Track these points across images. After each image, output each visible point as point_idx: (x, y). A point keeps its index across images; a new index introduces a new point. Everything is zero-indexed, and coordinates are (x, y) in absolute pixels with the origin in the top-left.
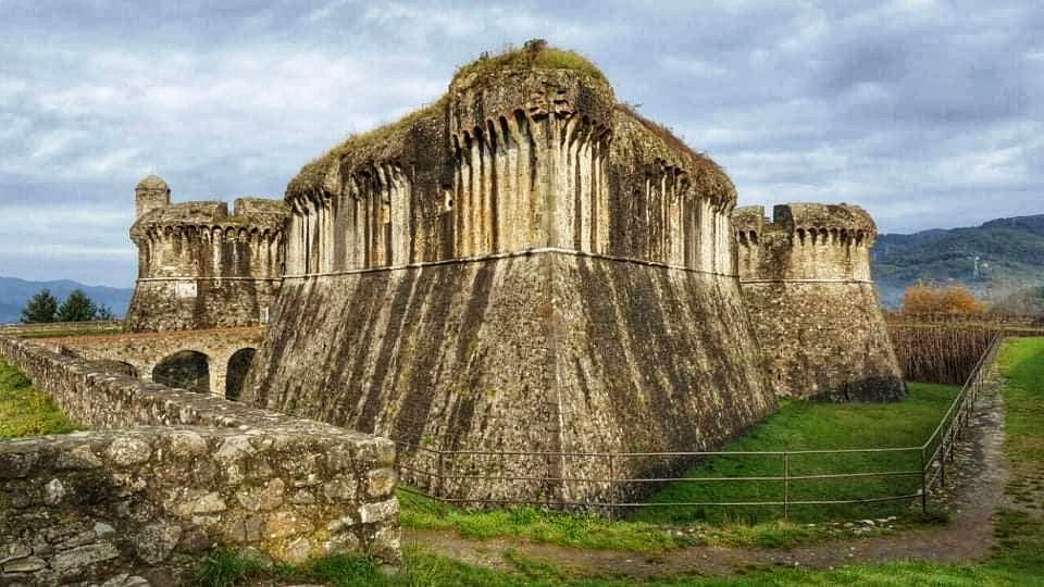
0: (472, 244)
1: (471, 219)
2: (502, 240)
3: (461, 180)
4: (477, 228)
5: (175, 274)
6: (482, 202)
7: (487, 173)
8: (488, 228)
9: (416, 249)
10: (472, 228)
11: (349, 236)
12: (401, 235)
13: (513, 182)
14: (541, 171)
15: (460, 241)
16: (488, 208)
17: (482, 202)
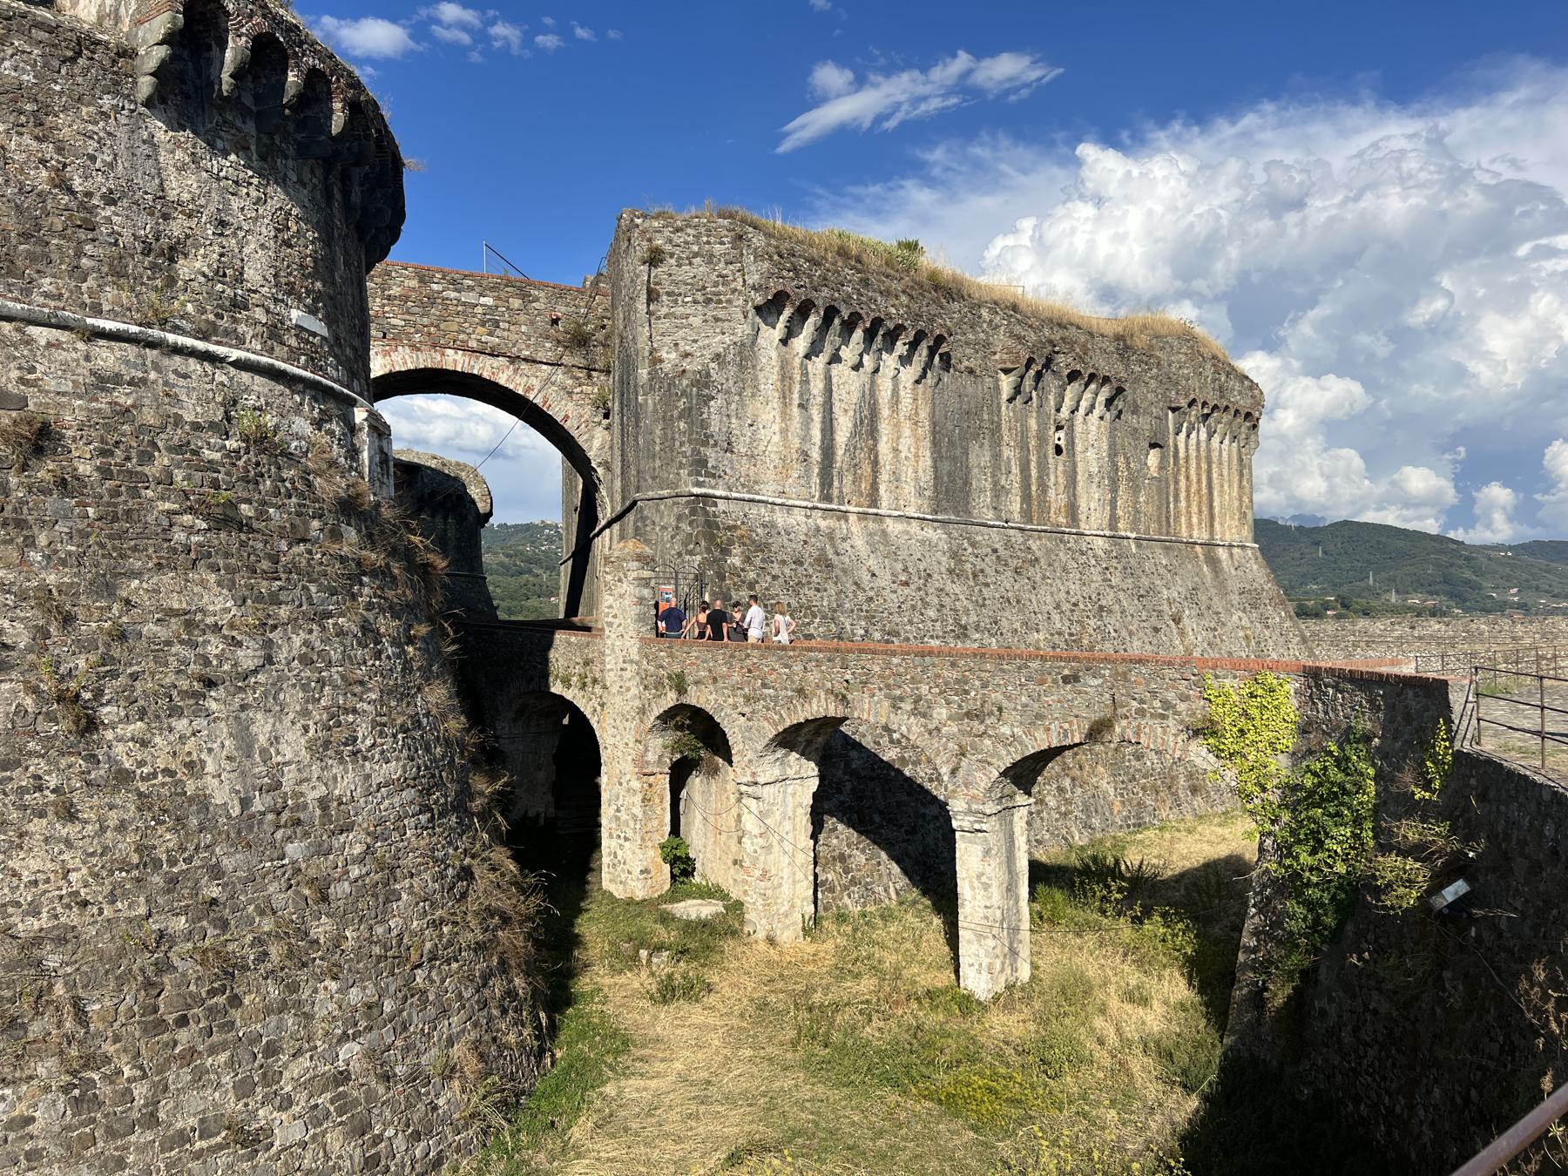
0: (1190, 526)
1: (1188, 496)
2: (1217, 527)
3: (1176, 446)
4: (1194, 509)
6: (1199, 481)
7: (1203, 454)
8: (1205, 509)
9: (1120, 512)
10: (1189, 506)
11: (979, 456)
12: (1094, 486)
13: (1225, 473)
14: (1246, 471)
15: (1177, 518)
16: (1204, 491)
17: (1199, 481)
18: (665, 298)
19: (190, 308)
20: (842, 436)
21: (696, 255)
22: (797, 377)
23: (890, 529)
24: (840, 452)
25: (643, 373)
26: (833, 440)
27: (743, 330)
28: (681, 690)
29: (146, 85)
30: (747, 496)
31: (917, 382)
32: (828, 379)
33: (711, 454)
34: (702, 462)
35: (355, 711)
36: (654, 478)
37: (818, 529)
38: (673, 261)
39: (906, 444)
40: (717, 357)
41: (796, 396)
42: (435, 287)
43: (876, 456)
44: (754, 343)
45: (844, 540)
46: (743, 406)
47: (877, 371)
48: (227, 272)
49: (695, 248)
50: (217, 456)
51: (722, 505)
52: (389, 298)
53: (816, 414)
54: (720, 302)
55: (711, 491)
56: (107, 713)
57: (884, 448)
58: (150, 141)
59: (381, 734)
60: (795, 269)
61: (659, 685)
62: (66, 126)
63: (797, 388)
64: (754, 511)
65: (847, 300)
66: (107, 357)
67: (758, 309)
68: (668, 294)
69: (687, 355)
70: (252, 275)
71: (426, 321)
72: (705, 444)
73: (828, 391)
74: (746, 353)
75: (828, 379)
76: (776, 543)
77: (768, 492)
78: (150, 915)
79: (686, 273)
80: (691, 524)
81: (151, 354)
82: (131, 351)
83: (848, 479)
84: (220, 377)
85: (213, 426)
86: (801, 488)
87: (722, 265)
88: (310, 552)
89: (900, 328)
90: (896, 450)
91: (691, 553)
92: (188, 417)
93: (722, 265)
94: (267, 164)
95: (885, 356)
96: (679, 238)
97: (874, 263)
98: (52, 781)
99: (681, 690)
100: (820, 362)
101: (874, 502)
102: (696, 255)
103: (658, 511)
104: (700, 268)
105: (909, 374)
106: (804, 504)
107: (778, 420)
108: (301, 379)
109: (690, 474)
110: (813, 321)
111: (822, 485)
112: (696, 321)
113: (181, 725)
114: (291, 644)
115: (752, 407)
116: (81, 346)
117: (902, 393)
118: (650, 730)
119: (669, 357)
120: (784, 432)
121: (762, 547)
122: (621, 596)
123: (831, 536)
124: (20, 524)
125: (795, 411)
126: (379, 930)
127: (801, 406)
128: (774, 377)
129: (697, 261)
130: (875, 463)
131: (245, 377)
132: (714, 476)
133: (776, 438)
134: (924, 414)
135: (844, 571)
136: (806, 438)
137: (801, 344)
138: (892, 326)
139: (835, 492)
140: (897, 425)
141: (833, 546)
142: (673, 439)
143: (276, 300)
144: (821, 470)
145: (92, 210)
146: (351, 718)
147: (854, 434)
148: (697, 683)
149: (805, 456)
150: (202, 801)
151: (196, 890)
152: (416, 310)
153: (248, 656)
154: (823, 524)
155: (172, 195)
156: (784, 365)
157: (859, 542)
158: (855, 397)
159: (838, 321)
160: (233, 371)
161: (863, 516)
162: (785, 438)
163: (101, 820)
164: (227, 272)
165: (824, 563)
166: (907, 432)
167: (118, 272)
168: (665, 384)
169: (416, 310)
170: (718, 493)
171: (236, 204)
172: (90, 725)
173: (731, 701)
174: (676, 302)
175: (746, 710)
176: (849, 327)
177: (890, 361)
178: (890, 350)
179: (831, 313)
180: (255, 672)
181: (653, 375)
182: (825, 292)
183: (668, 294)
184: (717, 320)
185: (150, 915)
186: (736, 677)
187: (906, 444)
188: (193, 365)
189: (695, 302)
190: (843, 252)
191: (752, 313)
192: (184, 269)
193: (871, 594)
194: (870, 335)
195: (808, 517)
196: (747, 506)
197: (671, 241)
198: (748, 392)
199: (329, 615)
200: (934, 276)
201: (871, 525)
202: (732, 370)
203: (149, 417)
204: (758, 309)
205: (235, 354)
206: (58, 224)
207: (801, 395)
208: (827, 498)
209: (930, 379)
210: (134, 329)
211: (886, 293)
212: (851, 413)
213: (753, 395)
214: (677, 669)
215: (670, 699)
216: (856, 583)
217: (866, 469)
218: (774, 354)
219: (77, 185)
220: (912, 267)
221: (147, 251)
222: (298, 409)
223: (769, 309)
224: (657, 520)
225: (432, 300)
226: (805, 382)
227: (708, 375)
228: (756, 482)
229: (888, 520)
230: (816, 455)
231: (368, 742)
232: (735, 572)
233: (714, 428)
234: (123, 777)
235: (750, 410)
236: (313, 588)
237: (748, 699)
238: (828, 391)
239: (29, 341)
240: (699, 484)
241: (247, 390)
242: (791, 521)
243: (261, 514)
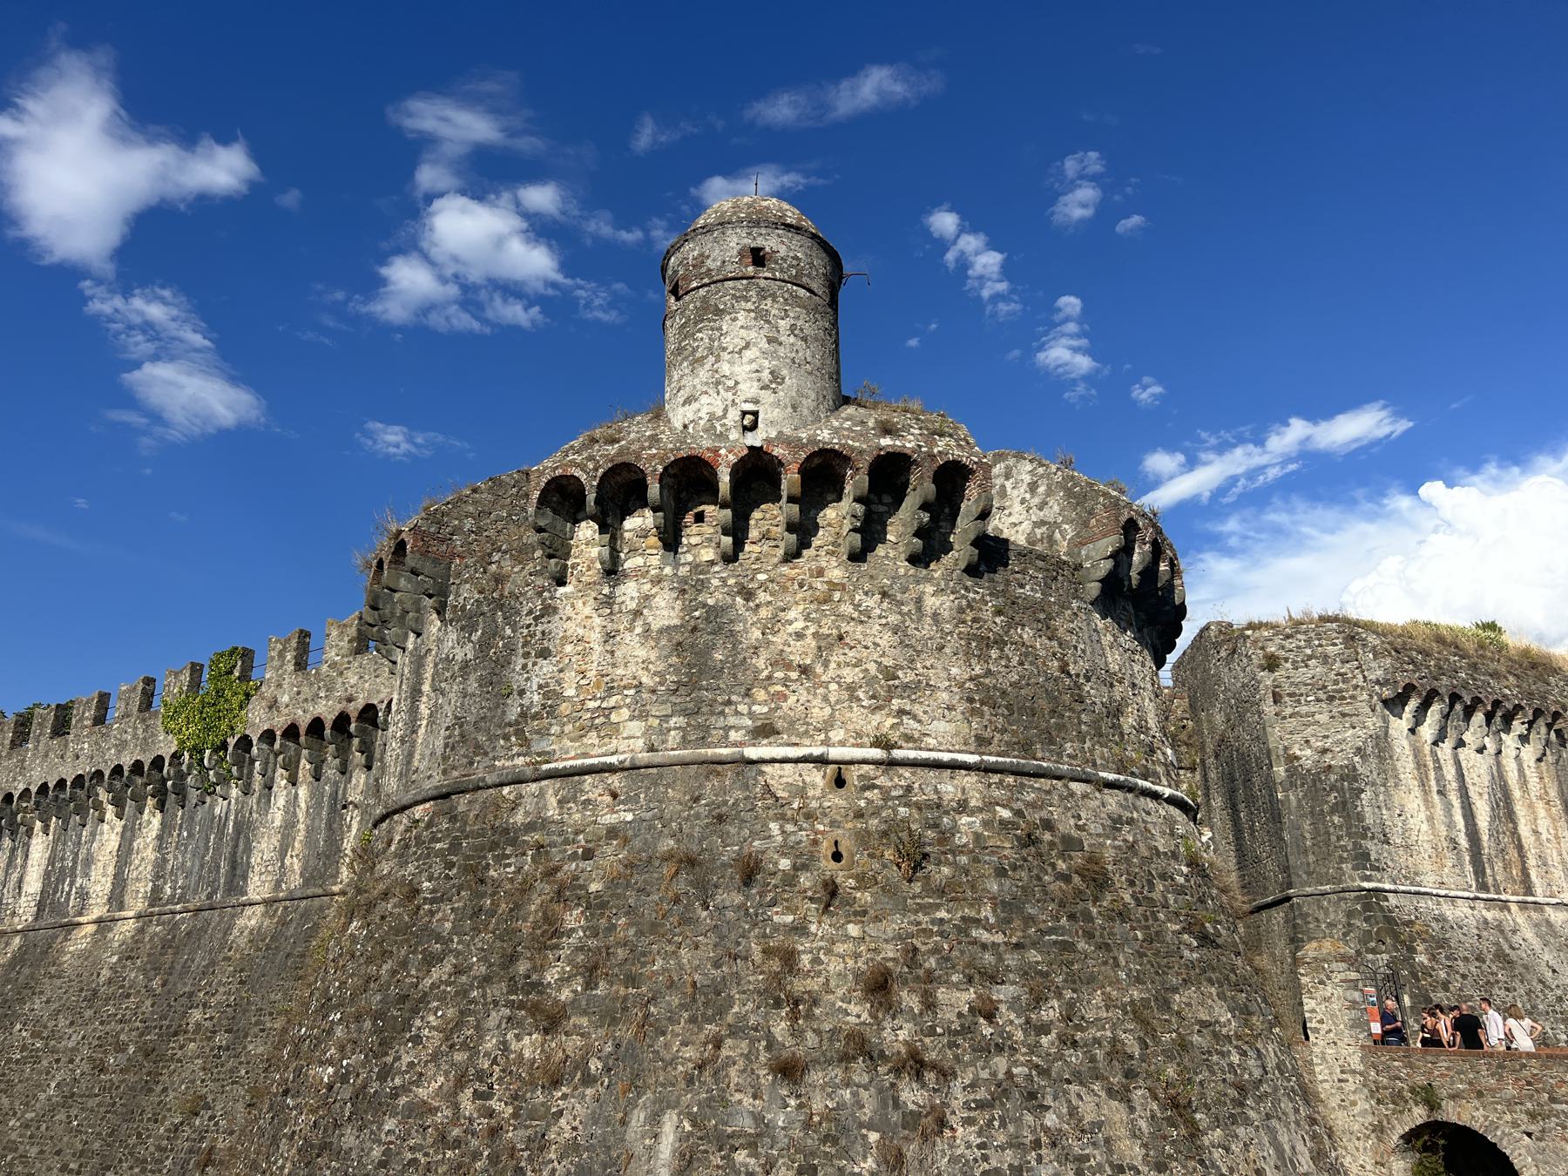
18: (1287, 699)
20: (1483, 821)
21: (1310, 658)
22: (1431, 765)
23: (1552, 918)
24: (1485, 838)
25: (1280, 771)
26: (1475, 825)
27: (1373, 723)
28: (1432, 1105)
29: (1094, 589)
30: (1413, 889)
31: (1539, 760)
32: (1458, 763)
33: (1371, 846)
34: (1366, 856)
36: (1309, 874)
37: (1486, 922)
38: (1288, 665)
39: (1544, 825)
40: (1358, 751)
41: (1433, 783)
43: (1519, 840)
44: (1386, 734)
45: (1514, 932)
46: (1390, 796)
47: (1500, 752)
49: (1309, 651)
51: (1393, 900)
53: (1454, 798)
54: (1344, 698)
55: (1380, 885)
57: (1524, 830)
60: (1413, 662)
61: (1397, 1098)
62: (1061, 625)
63: (1432, 775)
64: (1425, 904)
65: (1465, 686)
67: (1385, 702)
68: (1290, 695)
69: (1325, 751)
72: (1364, 837)
73: (1460, 776)
74: (1382, 744)
75: (1458, 763)
76: (1454, 937)
77: (1429, 883)
79: (1303, 674)
80: (1367, 920)
83: (1499, 866)
86: (1458, 879)
87: (1338, 664)
89: (1518, 708)
90: (1536, 832)
91: (1373, 951)
93: (1338, 664)
95: (1503, 736)
96: (1286, 644)
97: (1470, 647)
99: (1432, 1105)
100: (1447, 747)
101: (1529, 890)
102: (1310, 658)
103: (1320, 907)
104: (1317, 669)
105: (1529, 753)
106: (1466, 894)
107: (1423, 808)
109: (1355, 868)
110: (1435, 710)
111: (1476, 873)
112: (1323, 718)
115: (1398, 796)
117: (1527, 772)
118: (1393, 1151)
119: (1307, 756)
120: (1430, 819)
121: (1442, 943)
122: (1325, 999)
123: (1500, 928)
124: (1107, 947)
125: (1436, 797)
127: (1439, 792)
128: (1411, 766)
129: (1312, 662)
130: (1520, 847)
132: (1378, 869)
133: (1425, 827)
134: (1553, 793)
135: (1526, 967)
136: (1451, 825)
137: (1427, 731)
138: (1510, 707)
139: (1490, 881)
140: (1531, 806)
141: (1506, 939)
142: (1328, 833)
144: (1472, 857)
145: (1079, 687)
147: (1494, 818)
148: (1453, 1097)
149: (1454, 842)
154: (1489, 915)
156: (1417, 752)
157: (1529, 934)
158: (1486, 780)
159: (1462, 705)
161: (1523, 905)
162: (1433, 826)
165: (1501, 956)
166: (1542, 813)
168: (1313, 782)
170: (1387, 886)
172: (1195, 1133)
173: (1508, 1117)
174: (1299, 701)
175: (1532, 1128)
176: (1469, 712)
177: (1510, 740)
178: (1508, 730)
179: (1455, 698)
181: (1292, 772)
182: (1445, 680)
183: (1290, 695)
184: (1344, 715)
186: (1511, 1091)
187: (1544, 825)
189: (1318, 700)
190: (1440, 640)
191: (1379, 706)
193: (1559, 992)
194: (1489, 717)
195: (1472, 908)
196: (1415, 899)
197: (1283, 648)
198: (1391, 783)
200: (1526, 653)
201: (1534, 915)
202: (1373, 761)
204: (1385, 702)
207: (1438, 781)
208: (1483, 887)
209: (1550, 758)
211: (1495, 675)
212: (1486, 797)
213: (1396, 785)
214: (1421, 1080)
215: (1419, 1115)
216: (1540, 981)
217: (1513, 854)
218: (1405, 743)
219: (1072, 669)
220: (1502, 647)
223: (1395, 704)
224: (1322, 917)
226: (1438, 768)
227: (1355, 769)
228: (1416, 874)
229: (1547, 908)
230: (1463, 842)
232: (1427, 972)
233: (1369, 821)
235: (1396, 799)
237: (1533, 1116)
238: (1460, 776)
239: (1072, 794)
240: (1368, 879)
242: (1458, 913)
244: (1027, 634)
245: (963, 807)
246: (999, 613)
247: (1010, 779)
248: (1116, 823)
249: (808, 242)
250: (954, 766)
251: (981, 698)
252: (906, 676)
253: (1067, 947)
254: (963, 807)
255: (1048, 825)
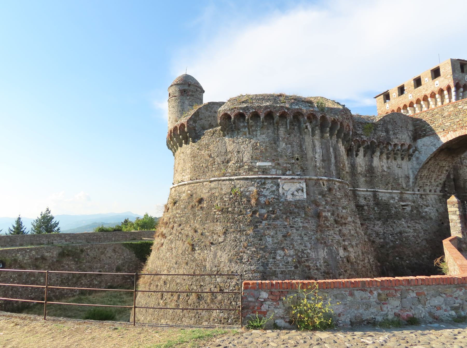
5: (273, 171)
19: (230, 171)
35: (244, 252)
42: (459, 107)
48: (240, 161)
50: (227, 199)
52: (444, 117)
56: (197, 248)
58: (225, 143)
59: (252, 259)
62: (211, 147)
66: (213, 185)
70: (245, 160)
71: (458, 120)
78: (191, 285)
81: (220, 182)
82: (217, 182)
84: (233, 183)
85: (228, 193)
88: (244, 217)
92: (223, 192)
94: (251, 134)
98: (187, 259)
108: (254, 178)
113: (206, 251)
114: (231, 237)
116: (210, 184)
126: (233, 303)
131: (238, 181)
143: (251, 163)
146: (242, 254)
150: (205, 267)
151: (200, 282)
152: (454, 117)
153: (221, 240)
155: (228, 151)
160: (235, 181)
163: (190, 266)
164: (240, 161)
167: (219, 169)
169: (454, 117)
171: (242, 147)
172: (193, 250)
180: (222, 242)
185: (191, 285)
188: (227, 182)
192: (230, 164)
199: (245, 231)
203: (217, 194)
205: (236, 177)
206: (210, 164)
210: (216, 179)
219: (213, 156)
221: (223, 162)
222: (253, 185)
225: (459, 112)
231: (246, 260)
234: (194, 260)
236: (241, 225)
241: (238, 184)
243: (234, 210)
244: (203, 152)
245: (184, 192)
246: (198, 149)
247: (193, 185)
248: (211, 189)
249: (174, 86)
250: (185, 184)
251: (195, 168)
252: (184, 168)
253: (189, 217)
254: (184, 192)
255: (196, 193)
